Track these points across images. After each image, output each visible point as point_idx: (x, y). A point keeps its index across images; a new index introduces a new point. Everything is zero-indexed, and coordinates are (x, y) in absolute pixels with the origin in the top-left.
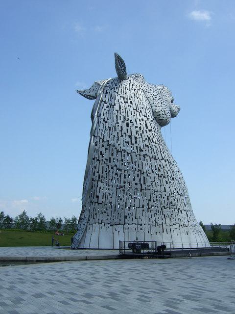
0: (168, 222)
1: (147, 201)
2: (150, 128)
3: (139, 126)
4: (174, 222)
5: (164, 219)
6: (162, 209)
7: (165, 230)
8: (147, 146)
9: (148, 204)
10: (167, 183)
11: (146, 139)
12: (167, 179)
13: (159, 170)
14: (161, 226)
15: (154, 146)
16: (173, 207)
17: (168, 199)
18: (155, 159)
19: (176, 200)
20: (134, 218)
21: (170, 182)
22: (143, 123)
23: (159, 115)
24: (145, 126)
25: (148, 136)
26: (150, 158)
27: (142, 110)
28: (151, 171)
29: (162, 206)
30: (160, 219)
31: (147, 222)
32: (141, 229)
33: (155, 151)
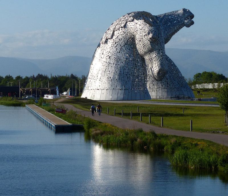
14: (152, 89)
30: (152, 86)
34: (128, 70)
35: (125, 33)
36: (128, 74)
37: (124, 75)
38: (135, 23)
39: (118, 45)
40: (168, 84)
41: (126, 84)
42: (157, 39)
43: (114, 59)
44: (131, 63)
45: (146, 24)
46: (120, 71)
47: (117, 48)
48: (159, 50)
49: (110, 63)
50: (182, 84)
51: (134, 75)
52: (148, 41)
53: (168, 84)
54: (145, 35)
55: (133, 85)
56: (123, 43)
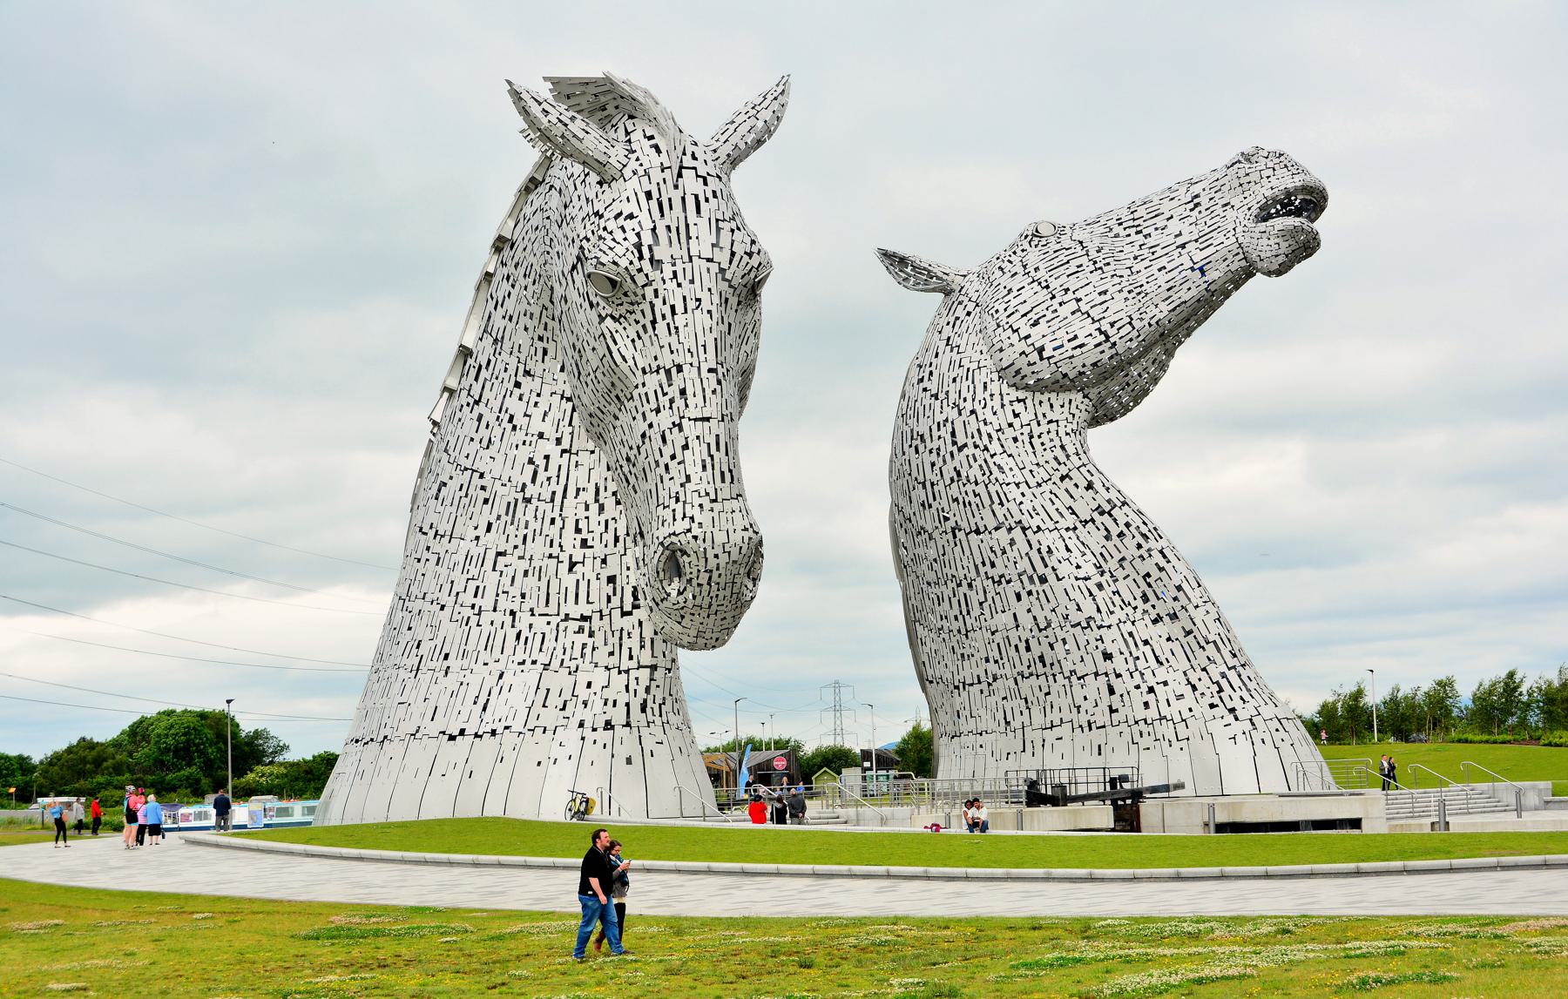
0: (1038, 719)
1: (984, 661)
2: (961, 440)
3: (935, 445)
4: (1055, 717)
5: (1026, 712)
6: (1016, 684)
7: (1029, 745)
8: (956, 500)
9: (986, 670)
10: (1019, 597)
11: (952, 480)
12: (1016, 586)
13: (993, 565)
15: (971, 497)
16: (1048, 669)
17: (1028, 649)
18: (978, 532)
19: (1058, 646)
20: (969, 716)
21: (1030, 593)
22: (945, 432)
23: (1018, 372)
24: (949, 441)
25: (955, 468)
26: (967, 534)
27: (952, 388)
28: (973, 574)
29: (1015, 671)
30: (1017, 713)
31: (992, 726)
32: (981, 746)
33: (974, 506)
34: (526, 573)
35: (513, 286)
36: (526, 607)
37: (498, 617)
38: (548, 186)
39: (488, 385)
40: (1112, 691)
41: (495, 691)
42: (641, 279)
43: (455, 502)
44: (547, 521)
45: (587, 170)
46: (478, 587)
47: (481, 408)
48: (668, 372)
49: (436, 534)
50: (1221, 690)
51: (567, 618)
52: (591, 305)
53: (1112, 691)
54: (574, 267)
55: (542, 692)
56: (513, 361)
